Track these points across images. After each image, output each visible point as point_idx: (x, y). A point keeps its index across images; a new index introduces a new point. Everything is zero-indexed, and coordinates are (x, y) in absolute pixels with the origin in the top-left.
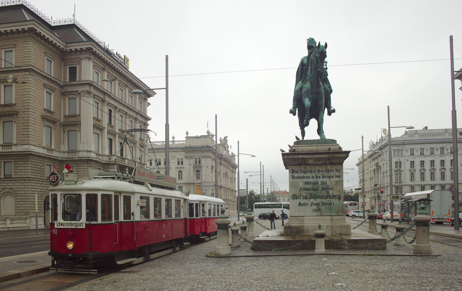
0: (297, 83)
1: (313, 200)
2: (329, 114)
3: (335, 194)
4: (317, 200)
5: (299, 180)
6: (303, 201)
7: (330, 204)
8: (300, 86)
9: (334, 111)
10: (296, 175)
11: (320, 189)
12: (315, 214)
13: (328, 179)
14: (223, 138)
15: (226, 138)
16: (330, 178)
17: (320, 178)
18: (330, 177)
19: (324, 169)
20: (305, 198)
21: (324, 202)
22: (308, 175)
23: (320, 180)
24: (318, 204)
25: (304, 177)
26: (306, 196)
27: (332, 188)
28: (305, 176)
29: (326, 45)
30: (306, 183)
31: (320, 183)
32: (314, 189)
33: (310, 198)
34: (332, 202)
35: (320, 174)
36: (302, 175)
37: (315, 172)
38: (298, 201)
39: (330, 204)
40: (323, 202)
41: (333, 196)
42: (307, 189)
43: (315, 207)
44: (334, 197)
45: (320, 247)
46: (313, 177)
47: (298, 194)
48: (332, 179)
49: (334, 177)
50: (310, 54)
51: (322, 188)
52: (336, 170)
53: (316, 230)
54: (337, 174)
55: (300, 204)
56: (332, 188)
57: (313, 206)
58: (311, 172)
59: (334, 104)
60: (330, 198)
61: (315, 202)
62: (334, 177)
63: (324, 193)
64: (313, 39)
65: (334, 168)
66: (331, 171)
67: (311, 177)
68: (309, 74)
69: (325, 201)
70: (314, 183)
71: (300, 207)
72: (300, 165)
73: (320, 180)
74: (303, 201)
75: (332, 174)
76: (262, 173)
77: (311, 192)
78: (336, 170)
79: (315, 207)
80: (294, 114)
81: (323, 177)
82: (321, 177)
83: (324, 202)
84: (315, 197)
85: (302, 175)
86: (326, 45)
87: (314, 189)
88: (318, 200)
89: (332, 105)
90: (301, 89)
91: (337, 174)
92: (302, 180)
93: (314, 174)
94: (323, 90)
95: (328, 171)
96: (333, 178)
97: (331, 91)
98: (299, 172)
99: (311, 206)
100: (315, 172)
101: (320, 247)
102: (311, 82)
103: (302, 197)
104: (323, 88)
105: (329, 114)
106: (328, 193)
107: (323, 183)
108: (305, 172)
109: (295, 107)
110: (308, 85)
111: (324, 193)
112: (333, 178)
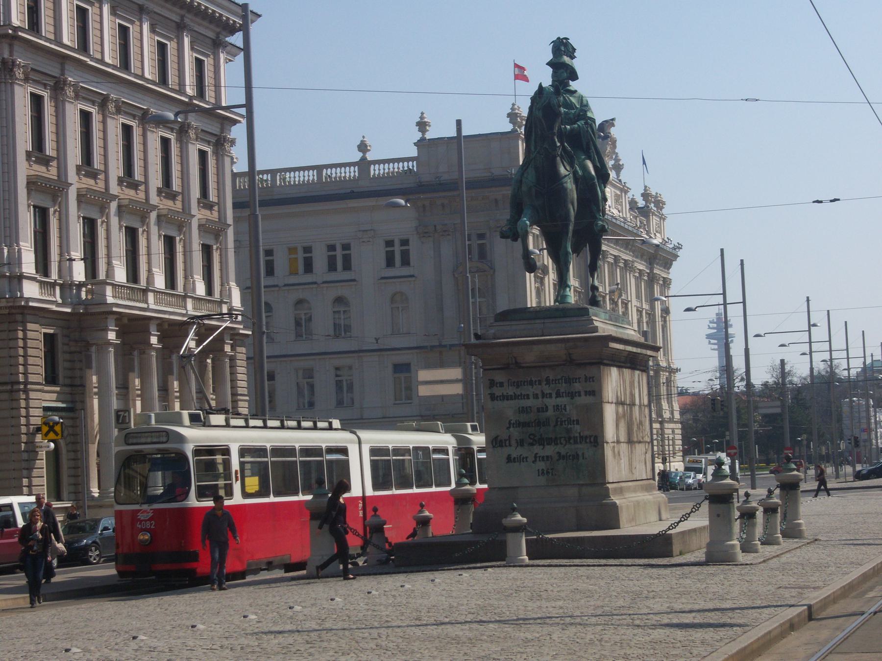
1: (537, 449)
3: (587, 433)
4: (547, 447)
5: (506, 403)
6: (515, 452)
7: (576, 457)
10: (498, 391)
12: (542, 480)
13: (569, 399)
16: (572, 398)
17: (551, 397)
18: (572, 395)
19: (559, 377)
20: (521, 443)
21: (563, 452)
23: (551, 402)
25: (515, 397)
27: (578, 421)
30: (524, 410)
31: (550, 408)
32: (539, 423)
33: (532, 444)
34: (580, 454)
36: (511, 391)
37: (540, 384)
38: (506, 451)
39: (576, 457)
40: (559, 453)
41: (581, 437)
43: (541, 465)
44: (583, 439)
46: (536, 396)
49: (583, 393)
51: (557, 422)
52: (586, 377)
55: (509, 459)
56: (578, 421)
57: (538, 462)
58: (531, 383)
60: (576, 442)
62: (583, 393)
65: (580, 373)
66: (578, 380)
67: (531, 397)
70: (538, 410)
72: (506, 367)
74: (515, 452)
75: (577, 386)
78: (586, 377)
81: (558, 395)
82: (554, 395)
84: (542, 441)
88: (550, 450)
92: (512, 402)
93: (537, 389)
96: (580, 395)
98: (506, 384)
99: (533, 462)
100: (540, 384)
103: (513, 442)
106: (568, 431)
107: (557, 408)
108: (518, 385)
112: (580, 395)
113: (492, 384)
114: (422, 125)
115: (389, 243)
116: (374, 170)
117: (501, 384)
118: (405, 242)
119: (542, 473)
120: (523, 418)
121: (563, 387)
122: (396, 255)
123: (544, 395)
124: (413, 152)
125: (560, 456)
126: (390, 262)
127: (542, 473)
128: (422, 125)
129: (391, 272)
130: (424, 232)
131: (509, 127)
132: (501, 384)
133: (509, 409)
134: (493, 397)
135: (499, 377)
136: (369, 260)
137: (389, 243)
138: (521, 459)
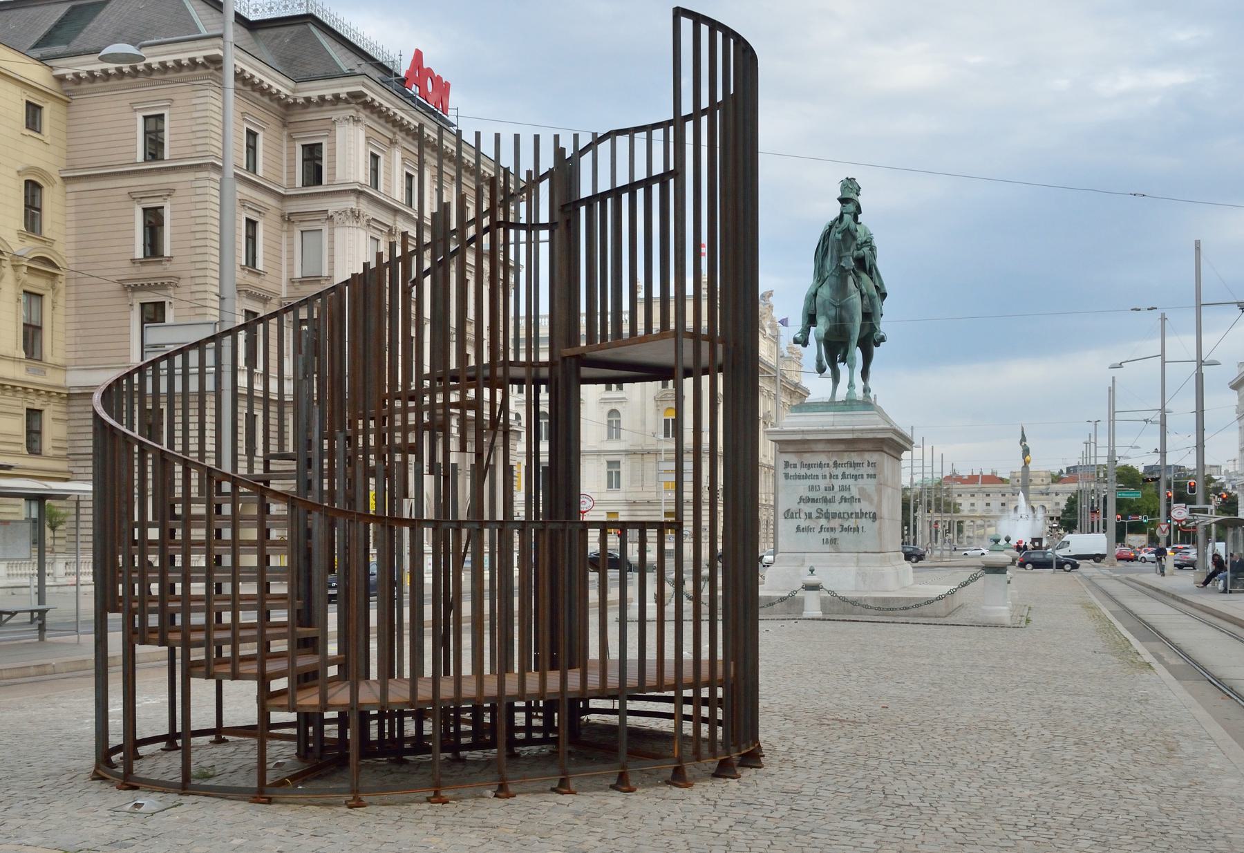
1: (823, 522)
5: (798, 482)
6: (804, 523)
10: (791, 472)
11: (838, 498)
12: (827, 547)
18: (856, 477)
20: (809, 516)
22: (814, 471)
23: (837, 483)
24: (832, 529)
25: (806, 477)
26: (810, 514)
28: (809, 473)
30: (812, 488)
31: (836, 488)
32: (825, 500)
33: (818, 518)
35: (839, 472)
36: (803, 471)
38: (795, 522)
39: (856, 530)
42: (813, 500)
43: (827, 535)
46: (824, 477)
47: (794, 507)
54: (871, 471)
55: (798, 528)
58: (820, 465)
60: (857, 517)
64: (851, 180)
79: (827, 535)
80: (805, 343)
81: (844, 476)
83: (846, 526)
84: (827, 516)
85: (803, 471)
87: (825, 500)
88: (835, 523)
90: (815, 295)
91: (871, 471)
93: (826, 471)
95: (853, 465)
97: (884, 296)
103: (803, 515)
107: (842, 488)
108: (809, 466)
109: (806, 332)
111: (844, 508)
113: (787, 464)
117: (795, 466)
119: (825, 541)
120: (811, 495)
127: (825, 541)
132: (795, 466)
133: (802, 488)
134: (787, 476)
135: (792, 459)
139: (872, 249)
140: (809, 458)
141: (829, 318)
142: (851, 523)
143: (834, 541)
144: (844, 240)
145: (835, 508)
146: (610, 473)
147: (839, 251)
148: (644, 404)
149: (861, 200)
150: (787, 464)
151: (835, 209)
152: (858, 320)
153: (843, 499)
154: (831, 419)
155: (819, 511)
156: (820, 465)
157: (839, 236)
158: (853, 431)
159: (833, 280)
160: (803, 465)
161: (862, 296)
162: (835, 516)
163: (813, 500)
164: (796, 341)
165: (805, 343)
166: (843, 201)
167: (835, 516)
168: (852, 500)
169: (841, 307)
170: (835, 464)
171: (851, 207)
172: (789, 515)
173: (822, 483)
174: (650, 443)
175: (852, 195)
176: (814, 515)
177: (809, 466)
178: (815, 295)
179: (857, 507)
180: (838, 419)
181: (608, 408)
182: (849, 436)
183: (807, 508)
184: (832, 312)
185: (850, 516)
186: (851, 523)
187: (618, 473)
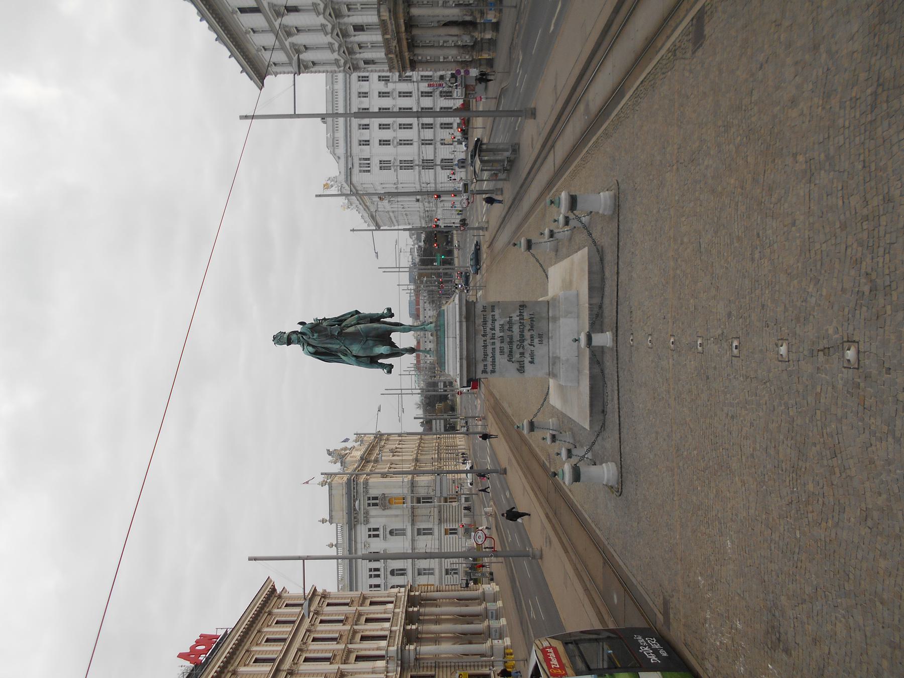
0: (343, 362)
2: (392, 315)
5: (497, 363)
6: (527, 359)
8: (354, 359)
9: (389, 310)
10: (490, 368)
11: (509, 333)
14: (330, 458)
15: (330, 453)
18: (494, 320)
20: (522, 354)
23: (498, 333)
25: (493, 357)
26: (521, 353)
28: (490, 355)
29: (301, 323)
30: (502, 352)
31: (501, 334)
32: (511, 342)
36: (489, 359)
38: (527, 364)
39: (532, 319)
42: (511, 352)
43: (536, 341)
44: (521, 315)
45: (604, 339)
46: (493, 343)
47: (517, 365)
48: (497, 317)
50: (299, 342)
53: (579, 346)
55: (532, 362)
58: (485, 346)
59: (380, 310)
60: (523, 319)
61: (529, 341)
63: (516, 329)
68: (336, 347)
69: (528, 327)
71: (535, 361)
73: (498, 333)
74: (527, 359)
76: (399, 392)
77: (514, 347)
79: (536, 341)
80: (391, 366)
81: (493, 329)
84: (522, 339)
85: (489, 359)
86: (302, 323)
87: (511, 342)
88: (527, 335)
89: (380, 312)
90: (357, 357)
93: (489, 341)
94: (362, 326)
97: (357, 312)
101: (604, 339)
102: (351, 344)
104: (358, 326)
105: (392, 315)
108: (486, 355)
109: (383, 366)
110: (356, 349)
111: (516, 329)
113: (484, 372)
114: (323, 521)
115: (370, 536)
116: (340, 541)
117: (485, 365)
118: (370, 530)
119: (541, 342)
120: (506, 350)
121: (489, 325)
122: (374, 533)
123: (493, 338)
124: (334, 525)
125: (532, 329)
126: (377, 536)
127: (541, 342)
128: (323, 521)
129: (381, 536)
130: (367, 522)
131: (327, 486)
132: (485, 365)
134: (493, 371)
135: (480, 367)
136: (377, 545)
137: (370, 536)
138: (532, 355)
139: (325, 319)
140: (480, 355)
141: (375, 345)
142: (527, 322)
143: (540, 336)
144: (319, 332)
145: (516, 337)
146: (424, 534)
147: (326, 336)
148: (387, 516)
149: (288, 331)
150: (484, 372)
151: (296, 348)
152: (375, 325)
153: (510, 329)
154: (451, 339)
155: (519, 347)
156: (485, 346)
157: (316, 335)
158: (461, 322)
159: (347, 342)
160: (485, 360)
161: (358, 324)
162: (522, 336)
163: (511, 352)
164: (390, 372)
165: (391, 366)
166: (289, 342)
167: (522, 336)
168: (510, 323)
169: (367, 336)
170: (483, 336)
171: (294, 337)
172: (521, 370)
173: (498, 345)
174: (407, 512)
175: (285, 336)
176: (521, 350)
177: (486, 355)
178: (357, 357)
179: (516, 318)
180: (451, 335)
181: (388, 536)
182: (464, 324)
183: (517, 356)
184: (371, 343)
185: (522, 324)
186: (527, 322)
187: (424, 529)
